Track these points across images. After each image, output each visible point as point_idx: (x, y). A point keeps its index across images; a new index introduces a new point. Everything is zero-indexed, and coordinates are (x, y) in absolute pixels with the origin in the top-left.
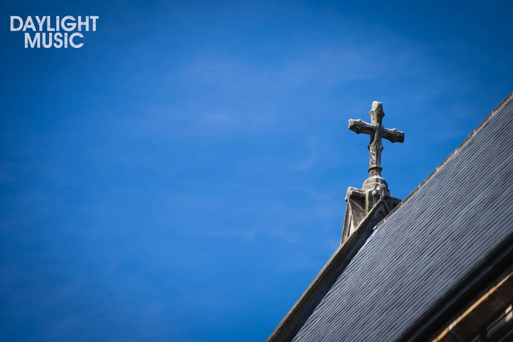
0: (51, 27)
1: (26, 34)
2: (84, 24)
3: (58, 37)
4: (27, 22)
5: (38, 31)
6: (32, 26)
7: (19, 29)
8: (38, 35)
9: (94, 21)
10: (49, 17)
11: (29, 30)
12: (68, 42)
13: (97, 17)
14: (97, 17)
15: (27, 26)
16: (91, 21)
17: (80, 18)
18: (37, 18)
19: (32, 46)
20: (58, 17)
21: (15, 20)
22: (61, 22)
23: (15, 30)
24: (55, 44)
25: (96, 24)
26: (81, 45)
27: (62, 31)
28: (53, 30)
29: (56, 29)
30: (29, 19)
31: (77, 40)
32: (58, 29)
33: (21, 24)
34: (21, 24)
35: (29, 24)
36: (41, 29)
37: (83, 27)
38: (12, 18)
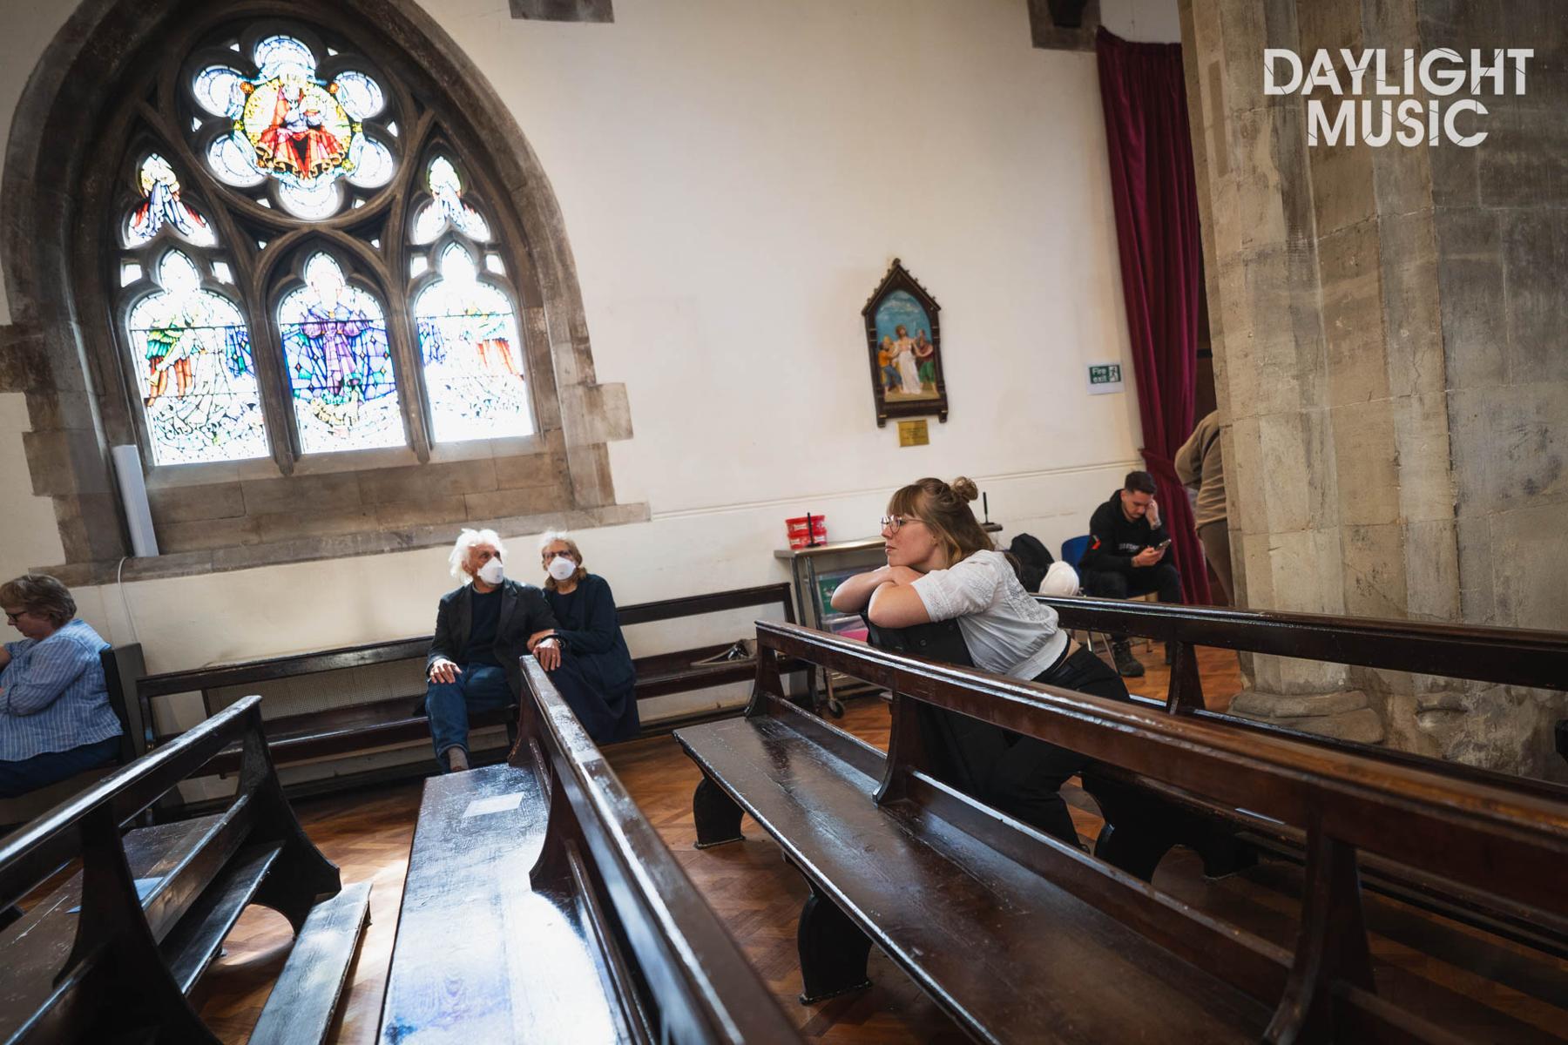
1: (1311, 103)
2: (1491, 72)
3: (1410, 113)
4: (1315, 68)
8: (1347, 108)
9: (1521, 65)
10: (1381, 54)
11: (1321, 92)
13: (1530, 53)
14: (1530, 53)
15: (1315, 79)
16: (1510, 64)
17: (1476, 54)
18: (1346, 54)
19: (1332, 139)
20: (1409, 53)
23: (1278, 91)
24: (1401, 136)
26: (1480, 138)
27: (1422, 95)
28: (1395, 90)
29: (1402, 90)
30: (1322, 57)
31: (1466, 123)
32: (1409, 89)
35: (1322, 72)
36: (1357, 89)
37: (1487, 83)
38: (1270, 55)
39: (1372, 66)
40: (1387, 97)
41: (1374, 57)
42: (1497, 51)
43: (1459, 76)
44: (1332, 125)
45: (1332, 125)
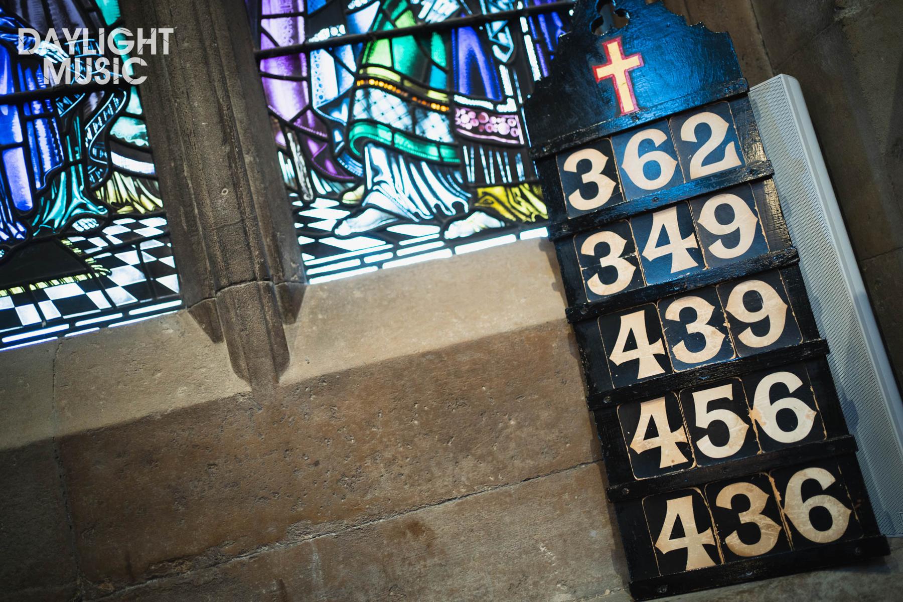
2: (149, 42)
9: (166, 38)
10: (86, 32)
13: (171, 30)
14: (171, 30)
16: (160, 37)
17: (140, 31)
18: (66, 31)
21: (27, 35)
27: (109, 54)
28: (94, 52)
29: (98, 52)
32: (101, 52)
36: (72, 50)
37: (147, 47)
38: (22, 31)
39: (81, 37)
40: (89, 56)
41: (82, 31)
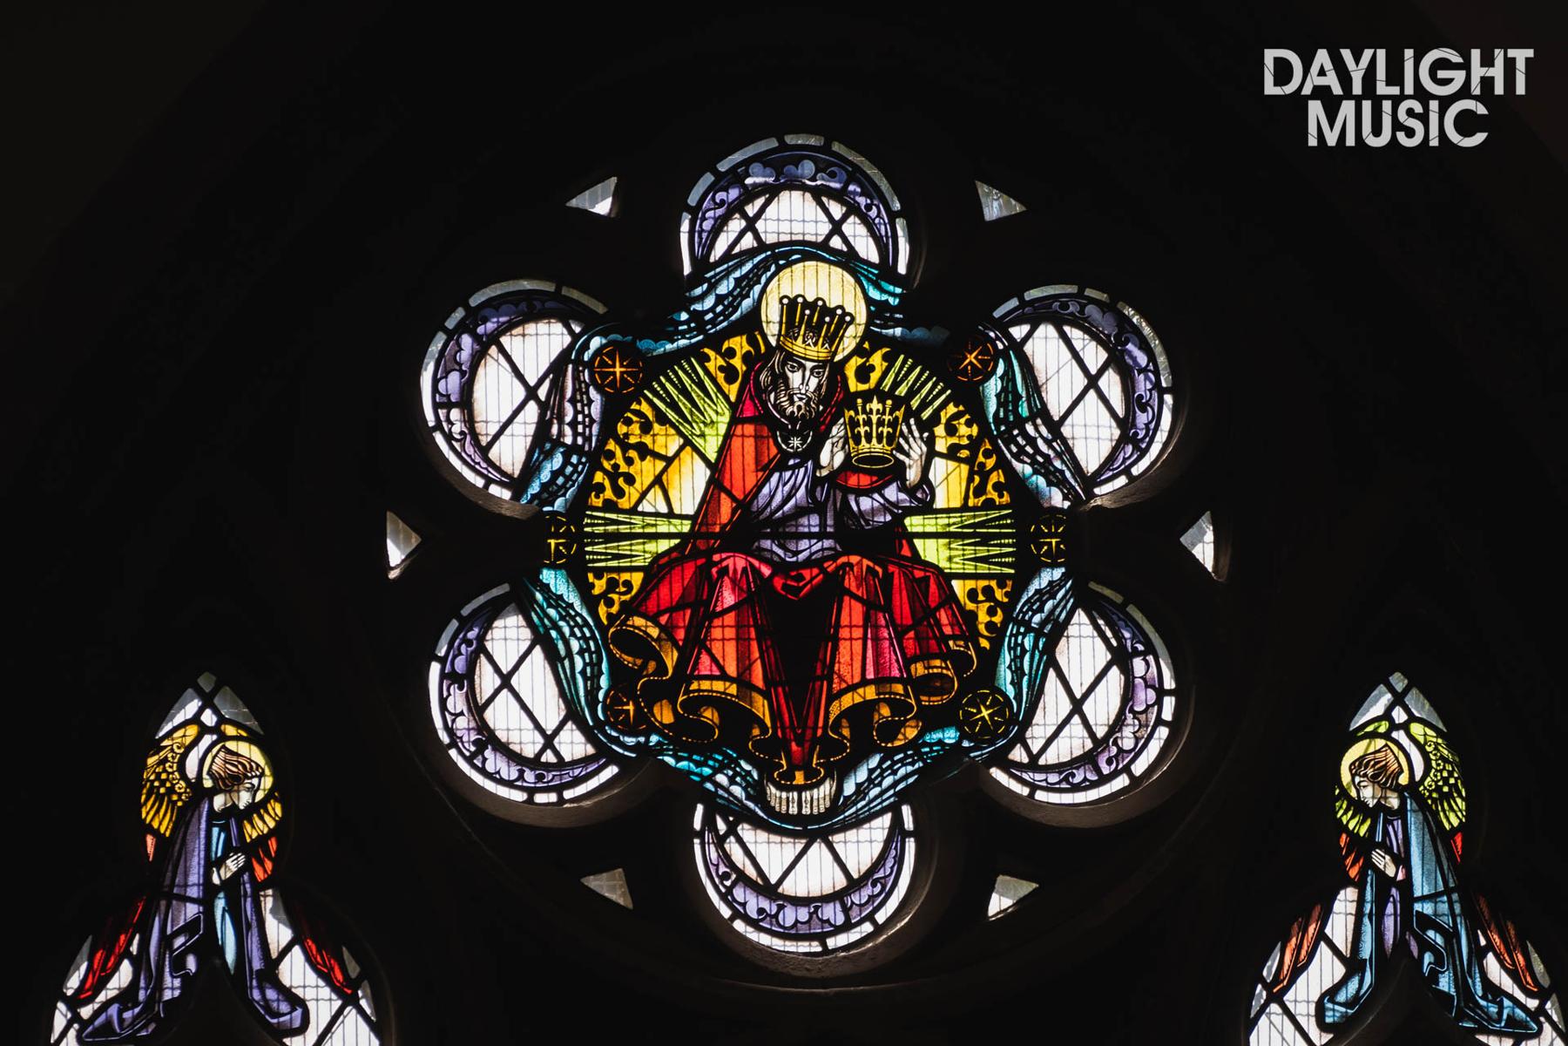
0: (1389, 83)
1: (1311, 103)
2: (1490, 72)
3: (1410, 113)
4: (1315, 69)
5: (1348, 94)
6: (1332, 81)
7: (1289, 89)
8: (1348, 108)
9: (1521, 66)
10: (1381, 53)
11: (1321, 93)
12: (1442, 128)
13: (1530, 53)
14: (1530, 53)
15: (1315, 80)
16: (1510, 64)
17: (1476, 54)
18: (1347, 54)
19: (1332, 139)
21: (1276, 59)
22: (1418, 68)
23: (1278, 91)
24: (1401, 136)
25: (1527, 74)
26: (1480, 138)
27: (1422, 95)
28: (1395, 91)
29: (1402, 90)
30: (1322, 57)
31: (1466, 123)
32: (1409, 89)
33: (1296, 73)
34: (1296, 73)
35: (1322, 73)
36: (1357, 89)
37: (1487, 83)
38: (1270, 55)
41: (1374, 58)
42: (1497, 51)
43: (1459, 77)
44: (1332, 126)
45: (1332, 126)
